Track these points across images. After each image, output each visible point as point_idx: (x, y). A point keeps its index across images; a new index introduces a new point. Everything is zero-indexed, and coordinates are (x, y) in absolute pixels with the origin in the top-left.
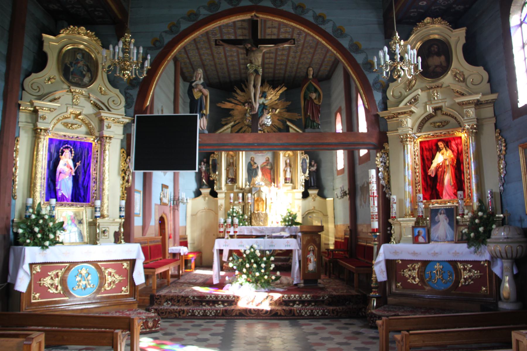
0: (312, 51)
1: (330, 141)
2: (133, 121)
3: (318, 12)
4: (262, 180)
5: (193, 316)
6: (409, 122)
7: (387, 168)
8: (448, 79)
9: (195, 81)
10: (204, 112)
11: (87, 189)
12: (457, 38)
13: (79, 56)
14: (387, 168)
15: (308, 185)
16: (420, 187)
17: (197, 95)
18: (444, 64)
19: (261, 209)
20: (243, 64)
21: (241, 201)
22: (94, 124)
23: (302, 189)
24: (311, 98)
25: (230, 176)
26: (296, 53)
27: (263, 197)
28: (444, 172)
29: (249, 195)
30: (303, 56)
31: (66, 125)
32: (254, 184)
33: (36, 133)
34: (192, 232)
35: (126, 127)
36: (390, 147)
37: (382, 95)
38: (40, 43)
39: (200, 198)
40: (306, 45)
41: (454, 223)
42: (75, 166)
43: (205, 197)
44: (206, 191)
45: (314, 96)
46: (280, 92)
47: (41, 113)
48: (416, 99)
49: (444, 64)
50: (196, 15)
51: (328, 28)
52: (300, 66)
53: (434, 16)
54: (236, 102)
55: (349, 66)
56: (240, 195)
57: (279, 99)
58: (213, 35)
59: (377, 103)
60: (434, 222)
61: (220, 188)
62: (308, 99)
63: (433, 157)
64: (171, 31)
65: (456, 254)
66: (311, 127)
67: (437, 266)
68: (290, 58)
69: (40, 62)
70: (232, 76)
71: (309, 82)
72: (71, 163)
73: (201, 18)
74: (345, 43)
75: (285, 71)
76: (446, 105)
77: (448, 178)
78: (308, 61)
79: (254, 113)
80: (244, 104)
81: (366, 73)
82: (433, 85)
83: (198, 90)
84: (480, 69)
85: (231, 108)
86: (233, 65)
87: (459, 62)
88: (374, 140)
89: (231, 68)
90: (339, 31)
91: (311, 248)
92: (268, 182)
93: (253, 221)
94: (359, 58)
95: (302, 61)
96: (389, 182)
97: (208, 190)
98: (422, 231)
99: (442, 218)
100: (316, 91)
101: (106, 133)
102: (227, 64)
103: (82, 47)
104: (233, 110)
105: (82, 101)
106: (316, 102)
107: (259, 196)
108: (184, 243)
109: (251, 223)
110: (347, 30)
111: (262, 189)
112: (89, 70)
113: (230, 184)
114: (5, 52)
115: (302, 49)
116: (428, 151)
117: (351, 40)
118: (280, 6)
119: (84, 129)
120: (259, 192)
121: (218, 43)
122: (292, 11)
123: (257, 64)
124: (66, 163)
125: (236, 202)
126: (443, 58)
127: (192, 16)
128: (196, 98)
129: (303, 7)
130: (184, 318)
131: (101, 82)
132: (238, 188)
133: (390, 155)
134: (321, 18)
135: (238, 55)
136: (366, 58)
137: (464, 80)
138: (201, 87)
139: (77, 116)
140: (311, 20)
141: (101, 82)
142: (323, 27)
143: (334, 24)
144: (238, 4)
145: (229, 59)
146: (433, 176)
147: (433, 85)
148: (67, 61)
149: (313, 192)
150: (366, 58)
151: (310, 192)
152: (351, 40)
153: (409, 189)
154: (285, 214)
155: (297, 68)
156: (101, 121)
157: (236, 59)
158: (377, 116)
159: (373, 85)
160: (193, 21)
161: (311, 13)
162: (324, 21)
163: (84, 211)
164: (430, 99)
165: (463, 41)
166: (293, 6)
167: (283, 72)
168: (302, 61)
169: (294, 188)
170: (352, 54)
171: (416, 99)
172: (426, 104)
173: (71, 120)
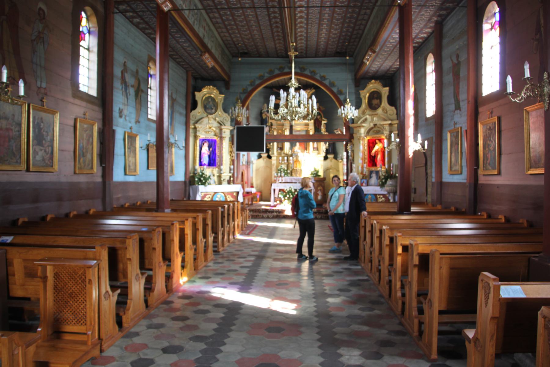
2: (235, 129)
3: (322, 74)
4: (299, 149)
5: (263, 218)
6: (363, 131)
7: (353, 151)
8: (380, 111)
11: (214, 160)
12: (385, 91)
13: (210, 100)
14: (353, 151)
15: (327, 152)
16: (366, 161)
19: (298, 167)
21: (286, 161)
22: (218, 131)
23: (324, 154)
25: (280, 146)
27: (300, 159)
28: (378, 154)
29: (291, 158)
31: (206, 132)
32: (294, 152)
33: (196, 137)
34: (257, 180)
35: (231, 131)
36: (355, 141)
38: (194, 96)
39: (261, 160)
41: (378, 177)
42: (209, 150)
43: (264, 159)
47: (198, 129)
48: (366, 120)
50: (263, 76)
51: (327, 82)
56: (286, 158)
60: (371, 177)
61: (273, 154)
63: (374, 147)
64: (251, 85)
65: (376, 191)
67: (370, 197)
69: (194, 106)
72: (207, 149)
73: (265, 78)
74: (335, 90)
76: (378, 123)
77: (379, 157)
82: (373, 113)
84: (393, 108)
87: (385, 103)
88: (347, 138)
91: (319, 188)
92: (303, 150)
93: (293, 174)
96: (353, 158)
97: (266, 155)
98: (365, 181)
99: (374, 175)
101: (224, 135)
103: (212, 96)
105: (212, 121)
107: (297, 159)
108: (252, 187)
109: (292, 175)
110: (336, 83)
111: (298, 154)
112: (214, 106)
113: (279, 151)
114: (184, 105)
116: (371, 144)
117: (338, 88)
119: (213, 133)
120: (297, 156)
122: (309, 74)
124: (205, 149)
125: (283, 162)
126: (378, 101)
127: (261, 77)
130: (259, 218)
131: (220, 112)
132: (284, 153)
133: (355, 145)
134: (324, 78)
137: (387, 113)
139: (210, 128)
141: (220, 112)
146: (373, 155)
147: (373, 113)
148: (205, 103)
149: (330, 156)
151: (329, 156)
152: (338, 88)
153: (360, 161)
154: (313, 170)
156: (221, 130)
158: (349, 127)
161: (318, 75)
163: (215, 170)
164: (372, 120)
165: (387, 94)
169: (319, 154)
172: (370, 122)
173: (208, 130)
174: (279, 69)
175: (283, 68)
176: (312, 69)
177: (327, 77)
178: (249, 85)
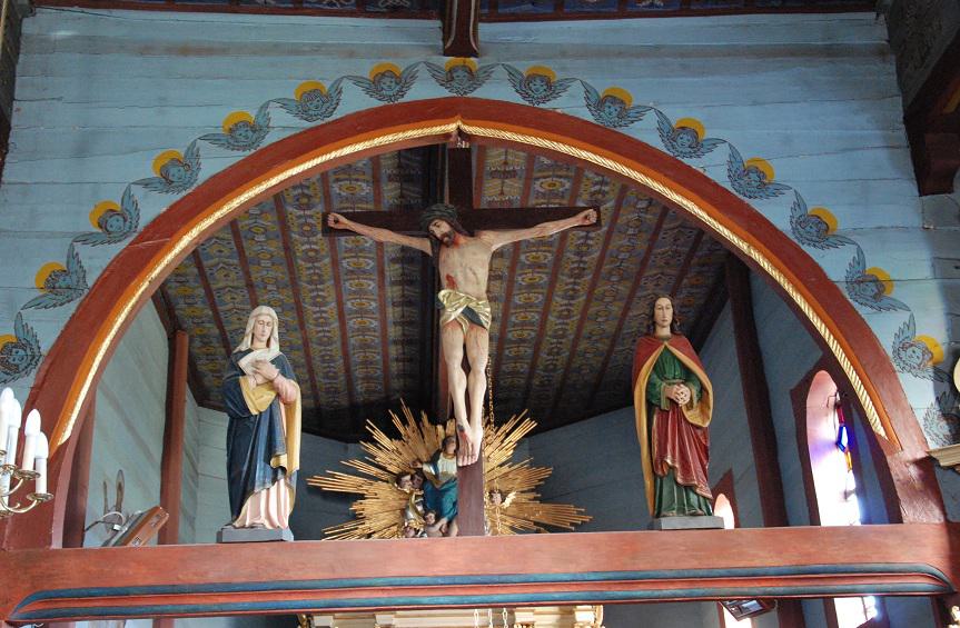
0: (624, 289)
1: (757, 562)
3: (676, 115)
9: (250, 351)
10: (284, 461)
17: (257, 400)
20: (395, 342)
24: (674, 403)
26: (572, 298)
30: (592, 310)
37: (936, 389)
40: (606, 268)
45: (683, 394)
46: (517, 435)
50: (257, 129)
52: (583, 345)
54: (374, 471)
55: (798, 290)
57: (512, 461)
58: (303, 234)
59: (920, 416)
62: (664, 405)
64: (166, 181)
66: (681, 511)
68: (551, 318)
70: (360, 387)
71: (661, 349)
73: (271, 139)
74: (778, 214)
75: (533, 367)
78: (610, 327)
79: (468, 462)
81: (864, 311)
83: (260, 380)
85: (351, 490)
86: (365, 346)
89: (357, 357)
90: (753, 176)
94: (834, 264)
95: (588, 327)
100: (688, 376)
102: (344, 344)
104: (362, 497)
106: (693, 416)
110: (779, 171)
115: (593, 286)
117: (799, 204)
118: (545, 99)
121: (331, 224)
123: (471, 289)
127: (235, 133)
128: (254, 412)
129: (622, 102)
135: (382, 310)
136: (860, 260)
138: (273, 372)
140: (655, 142)
142: (694, 163)
143: (734, 154)
144: (402, 93)
145: (352, 323)
150: (860, 260)
152: (799, 204)
155: (573, 353)
157: (375, 324)
159: (897, 352)
160: (244, 148)
161: (650, 119)
162: (698, 146)
166: (587, 98)
167: (524, 367)
168: (588, 327)
170: (806, 248)
174: (374, 85)
175: (403, 81)
176: (602, 87)
177: (708, 134)
178: (146, 184)
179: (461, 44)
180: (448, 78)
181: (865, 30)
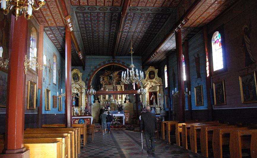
8: (154, 80)
12: (156, 71)
13: (76, 75)
18: (154, 77)
44: (97, 101)
46: (118, 72)
48: (148, 84)
49: (154, 77)
53: (152, 66)
57: (117, 75)
80: (107, 76)
101: (82, 91)
112: (78, 78)
113: (104, 99)
126: (153, 75)
131: (81, 80)
141: (81, 80)
171: (148, 84)
174: (108, 61)
179: (114, 58)
180: (113, 61)
181: (140, 57)
